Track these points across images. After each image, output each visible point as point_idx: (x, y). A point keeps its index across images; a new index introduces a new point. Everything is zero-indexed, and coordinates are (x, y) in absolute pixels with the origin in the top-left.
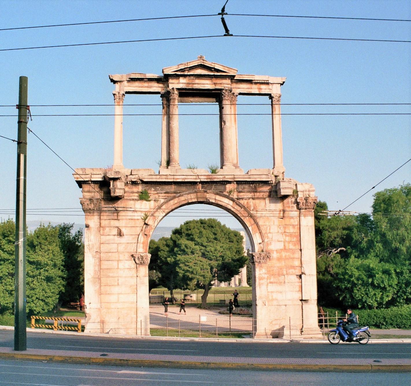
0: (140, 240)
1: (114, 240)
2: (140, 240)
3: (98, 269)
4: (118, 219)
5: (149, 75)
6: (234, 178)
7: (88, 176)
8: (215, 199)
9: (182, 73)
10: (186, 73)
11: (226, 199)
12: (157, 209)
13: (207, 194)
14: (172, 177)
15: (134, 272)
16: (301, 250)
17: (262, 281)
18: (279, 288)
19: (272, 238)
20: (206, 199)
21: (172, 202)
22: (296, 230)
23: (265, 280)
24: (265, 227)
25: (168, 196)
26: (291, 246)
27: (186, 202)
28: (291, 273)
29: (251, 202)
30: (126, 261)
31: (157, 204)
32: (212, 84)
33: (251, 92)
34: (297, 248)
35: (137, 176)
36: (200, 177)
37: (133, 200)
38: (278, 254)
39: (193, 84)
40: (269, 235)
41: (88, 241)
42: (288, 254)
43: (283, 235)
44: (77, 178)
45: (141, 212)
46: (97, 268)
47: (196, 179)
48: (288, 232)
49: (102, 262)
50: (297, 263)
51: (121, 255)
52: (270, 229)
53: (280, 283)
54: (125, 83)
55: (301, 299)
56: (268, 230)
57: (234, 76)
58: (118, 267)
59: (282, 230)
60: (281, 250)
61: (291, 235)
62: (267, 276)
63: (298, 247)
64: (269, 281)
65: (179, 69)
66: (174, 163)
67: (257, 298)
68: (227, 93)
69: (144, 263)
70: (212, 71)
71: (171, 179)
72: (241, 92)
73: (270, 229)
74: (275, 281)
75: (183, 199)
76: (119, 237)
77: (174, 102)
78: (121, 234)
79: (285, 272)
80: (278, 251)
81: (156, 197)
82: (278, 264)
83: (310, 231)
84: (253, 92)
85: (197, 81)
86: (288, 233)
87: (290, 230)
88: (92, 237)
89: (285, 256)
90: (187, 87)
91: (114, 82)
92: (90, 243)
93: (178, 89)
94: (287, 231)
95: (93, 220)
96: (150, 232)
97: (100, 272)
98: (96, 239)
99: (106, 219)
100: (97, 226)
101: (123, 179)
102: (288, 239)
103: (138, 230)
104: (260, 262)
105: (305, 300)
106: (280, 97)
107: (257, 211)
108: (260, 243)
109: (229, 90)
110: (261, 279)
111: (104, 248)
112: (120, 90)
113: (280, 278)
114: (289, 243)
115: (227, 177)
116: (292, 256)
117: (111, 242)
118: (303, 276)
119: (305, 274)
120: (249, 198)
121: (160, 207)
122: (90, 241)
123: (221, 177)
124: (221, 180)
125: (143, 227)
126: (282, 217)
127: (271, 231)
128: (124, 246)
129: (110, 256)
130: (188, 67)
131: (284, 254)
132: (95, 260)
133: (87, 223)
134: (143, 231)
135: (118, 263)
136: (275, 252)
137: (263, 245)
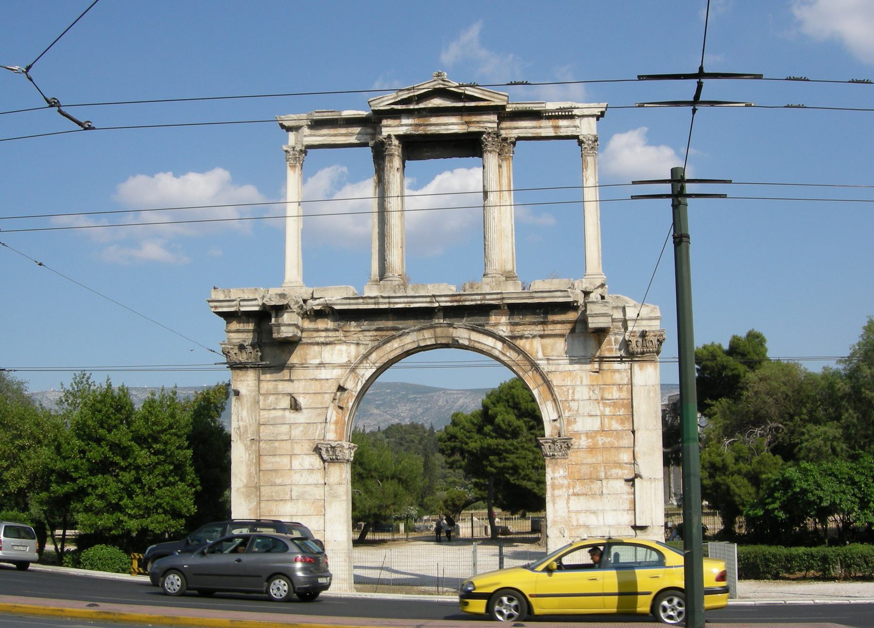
0: (331, 418)
1: (283, 417)
2: (331, 418)
3: (256, 470)
4: (290, 380)
5: (347, 113)
7: (233, 303)
8: (469, 339)
9: (404, 107)
10: (411, 107)
11: (490, 338)
12: (361, 362)
14: (387, 300)
15: (318, 478)
16: (633, 432)
17: (557, 492)
18: (593, 504)
19: (578, 410)
20: (453, 339)
21: (388, 347)
22: (625, 394)
23: (564, 490)
24: (565, 389)
25: (381, 336)
26: (615, 426)
27: (415, 345)
28: (615, 476)
29: (537, 343)
30: (305, 456)
31: (363, 350)
32: (462, 124)
33: (541, 133)
34: (625, 429)
35: (322, 300)
36: (438, 299)
37: (318, 344)
38: (590, 440)
39: (427, 125)
40: (572, 404)
41: (238, 421)
42: (607, 440)
43: (598, 403)
44: (216, 307)
45: (334, 366)
46: (253, 470)
47: (431, 302)
48: (610, 397)
49: (264, 459)
50: (626, 457)
51: (295, 445)
52: (573, 393)
53: (593, 495)
54: (306, 131)
55: (633, 524)
56: (570, 396)
57: (503, 107)
58: (291, 466)
59: (597, 394)
60: (596, 432)
61: (615, 404)
62: (569, 483)
63: (628, 426)
64: (571, 491)
65: (399, 99)
66: (391, 275)
68: (490, 139)
69: (337, 459)
70: (461, 100)
71: (385, 303)
72: (521, 135)
73: (573, 393)
74: (584, 492)
75: (409, 341)
76: (293, 413)
77: (391, 161)
78: (298, 407)
79: (602, 475)
80: (590, 434)
81: (359, 338)
82: (590, 460)
83: (652, 394)
84: (543, 135)
85: (433, 120)
86: (610, 400)
87: (612, 394)
88: (244, 414)
89: (603, 444)
90: (415, 131)
91: (289, 129)
93: (398, 137)
94: (607, 395)
95: (245, 383)
96: (348, 402)
97: (259, 477)
98: (252, 417)
99: (270, 380)
100: (254, 394)
101: (295, 307)
102: (607, 411)
103: (328, 398)
104: (554, 455)
105: (643, 528)
106: (596, 141)
107: (548, 359)
108: (555, 420)
109: (494, 134)
110: (554, 487)
111: (265, 432)
112: (296, 144)
113: (592, 486)
115: (488, 297)
116: (616, 445)
117: (278, 421)
118: (636, 480)
119: (641, 478)
120: (534, 337)
121: (366, 357)
122: (242, 419)
123: (478, 297)
124: (479, 302)
125: (336, 394)
126: (598, 370)
127: (576, 397)
128: (301, 428)
129: (276, 447)
130: (416, 94)
131: (601, 440)
132: (249, 455)
133: (235, 388)
134: (337, 401)
135: (291, 460)
136: (583, 438)
137: (560, 424)
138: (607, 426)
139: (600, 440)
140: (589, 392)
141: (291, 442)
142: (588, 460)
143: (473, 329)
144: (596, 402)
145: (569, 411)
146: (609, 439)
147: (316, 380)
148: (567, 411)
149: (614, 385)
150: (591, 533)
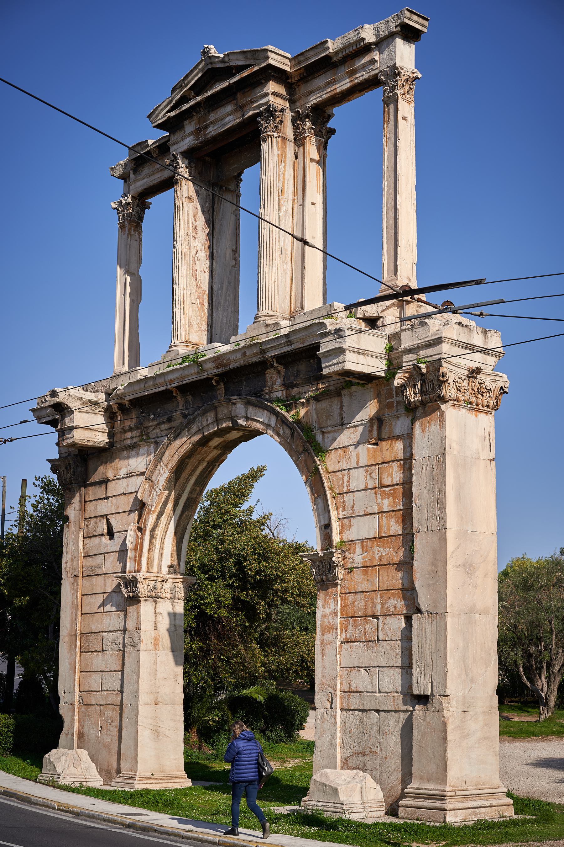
4: (106, 498)
6: (263, 352)
13: (234, 407)
17: (325, 637)
19: (353, 507)
43: (376, 493)
52: (348, 482)
56: (345, 485)
67: (317, 688)
73: (348, 482)
80: (365, 544)
89: (380, 559)
92: (69, 556)
95: (73, 505)
114: (391, 517)
132: (73, 594)
138: (386, 529)
139: (377, 552)
140: (366, 477)
141: (104, 577)
142: (363, 586)
143: (248, 403)
144: (373, 491)
145: (344, 510)
146: (387, 550)
147: (125, 494)
148: (341, 509)
149: (393, 461)
150: (363, 704)
